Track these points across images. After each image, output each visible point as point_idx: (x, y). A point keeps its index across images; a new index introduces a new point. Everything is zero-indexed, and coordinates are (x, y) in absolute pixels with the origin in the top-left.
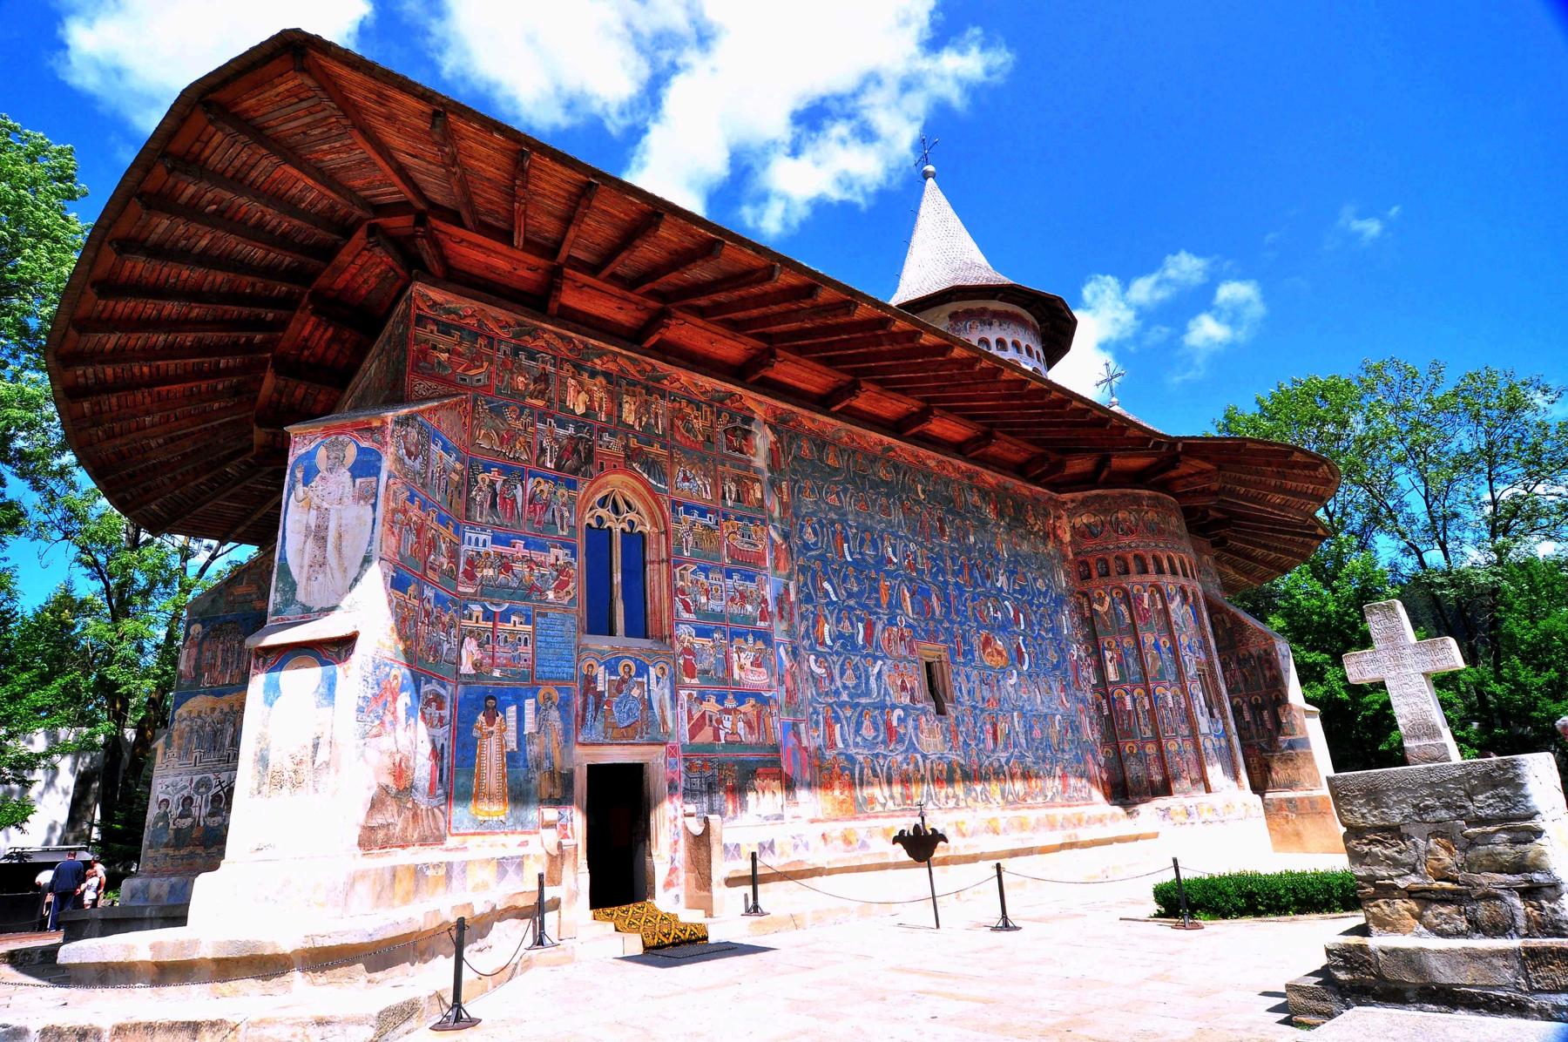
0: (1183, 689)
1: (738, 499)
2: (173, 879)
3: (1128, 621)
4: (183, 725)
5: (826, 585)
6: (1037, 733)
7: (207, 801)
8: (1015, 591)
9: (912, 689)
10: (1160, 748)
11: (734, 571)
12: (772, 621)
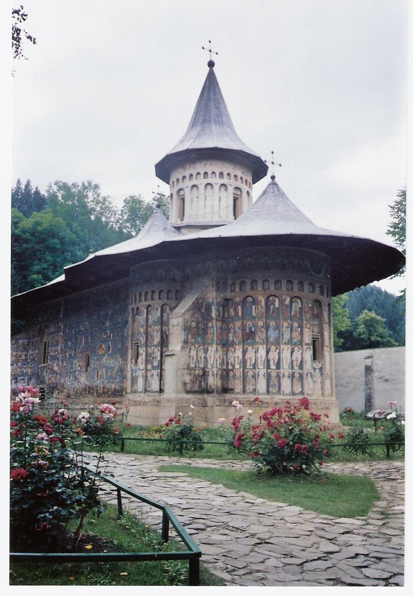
5: (69, 343)
6: (109, 374)
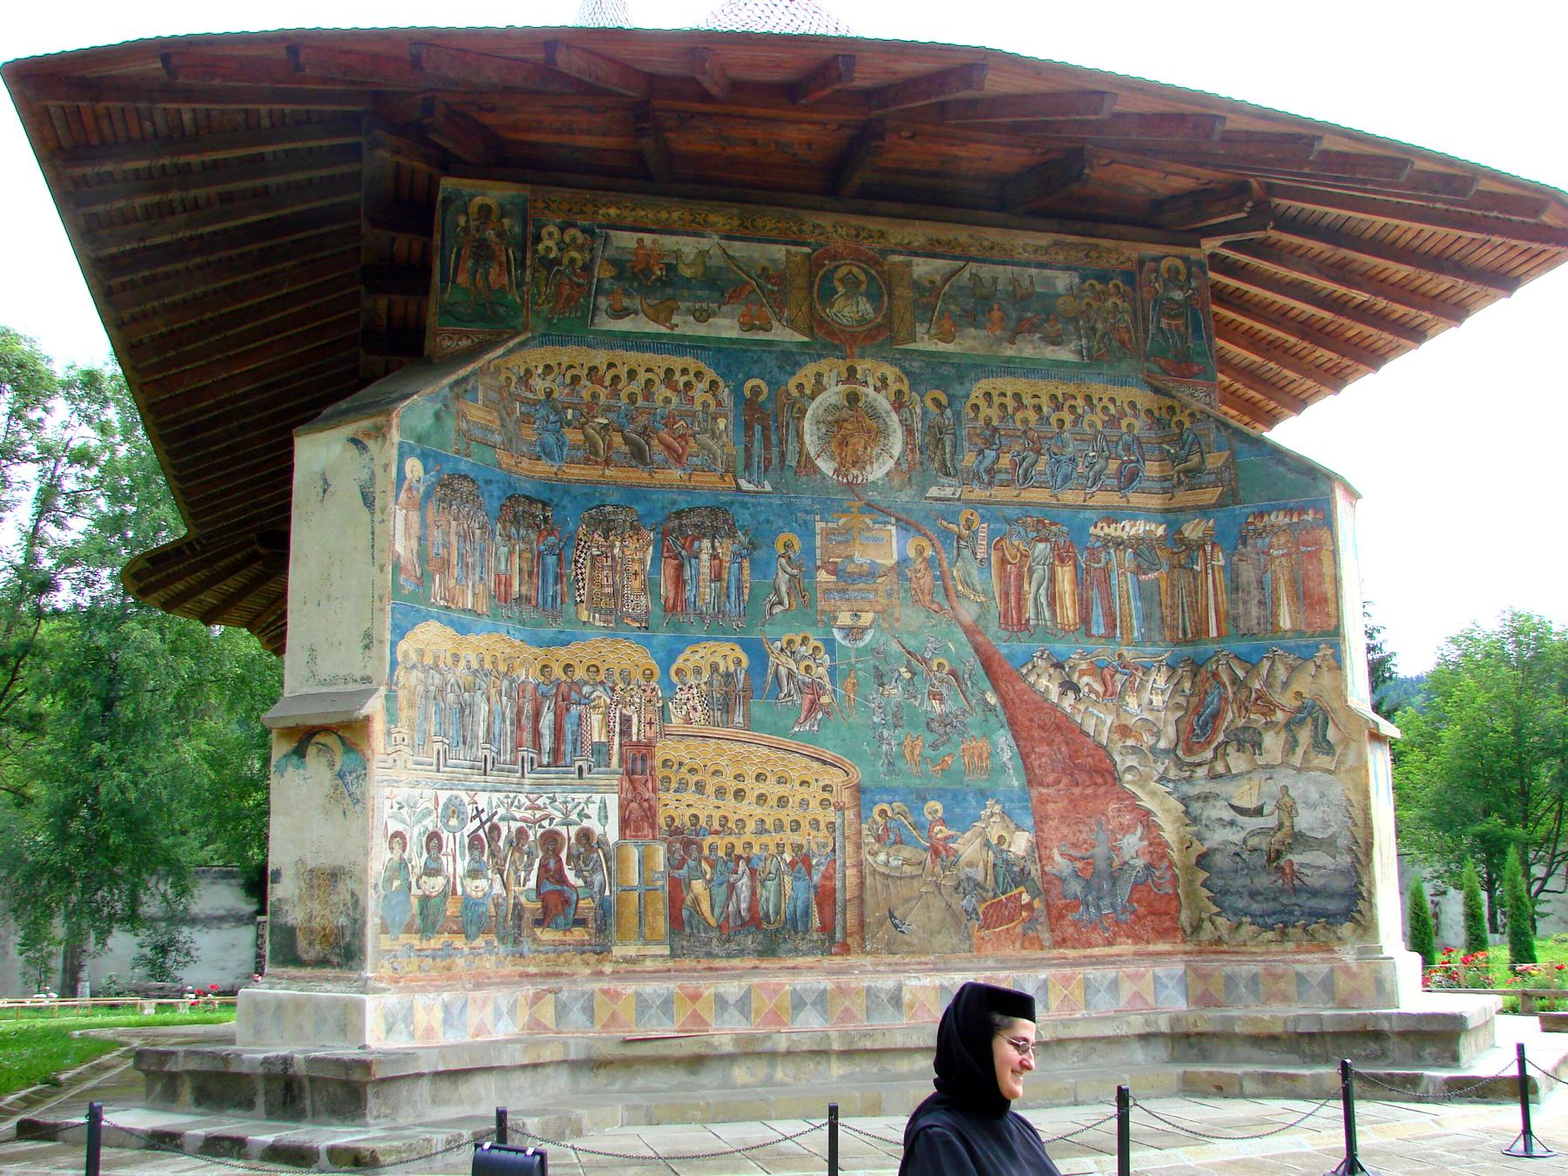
2: (446, 996)
4: (416, 675)
7: (462, 846)
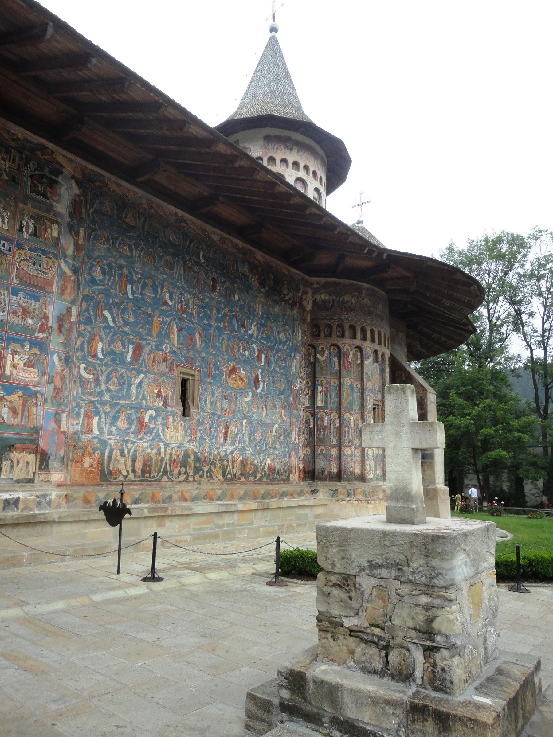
0: (362, 416)
1: (35, 234)
3: (337, 368)
5: (106, 313)
6: (258, 435)
8: (262, 338)
9: (166, 397)
10: (340, 451)
11: (21, 290)
12: (50, 334)
